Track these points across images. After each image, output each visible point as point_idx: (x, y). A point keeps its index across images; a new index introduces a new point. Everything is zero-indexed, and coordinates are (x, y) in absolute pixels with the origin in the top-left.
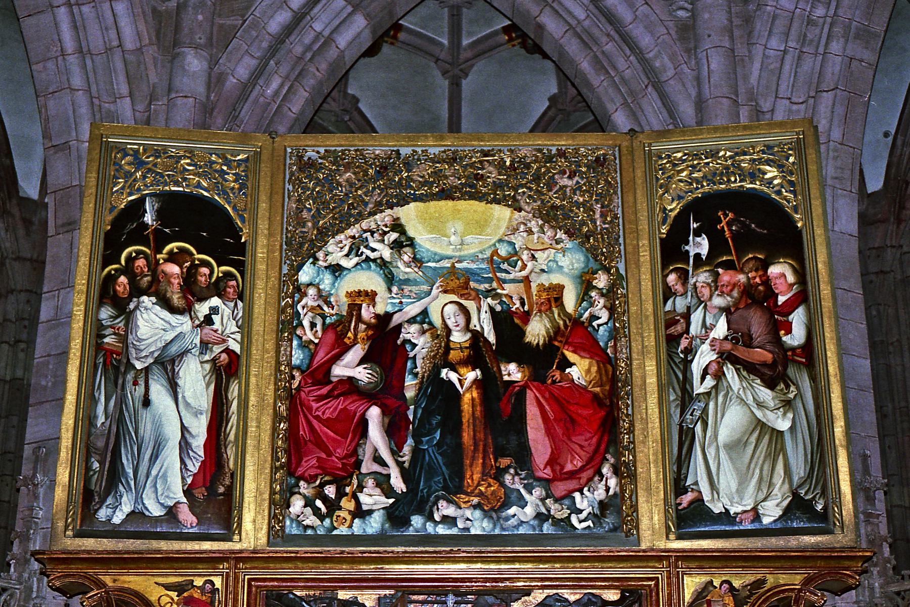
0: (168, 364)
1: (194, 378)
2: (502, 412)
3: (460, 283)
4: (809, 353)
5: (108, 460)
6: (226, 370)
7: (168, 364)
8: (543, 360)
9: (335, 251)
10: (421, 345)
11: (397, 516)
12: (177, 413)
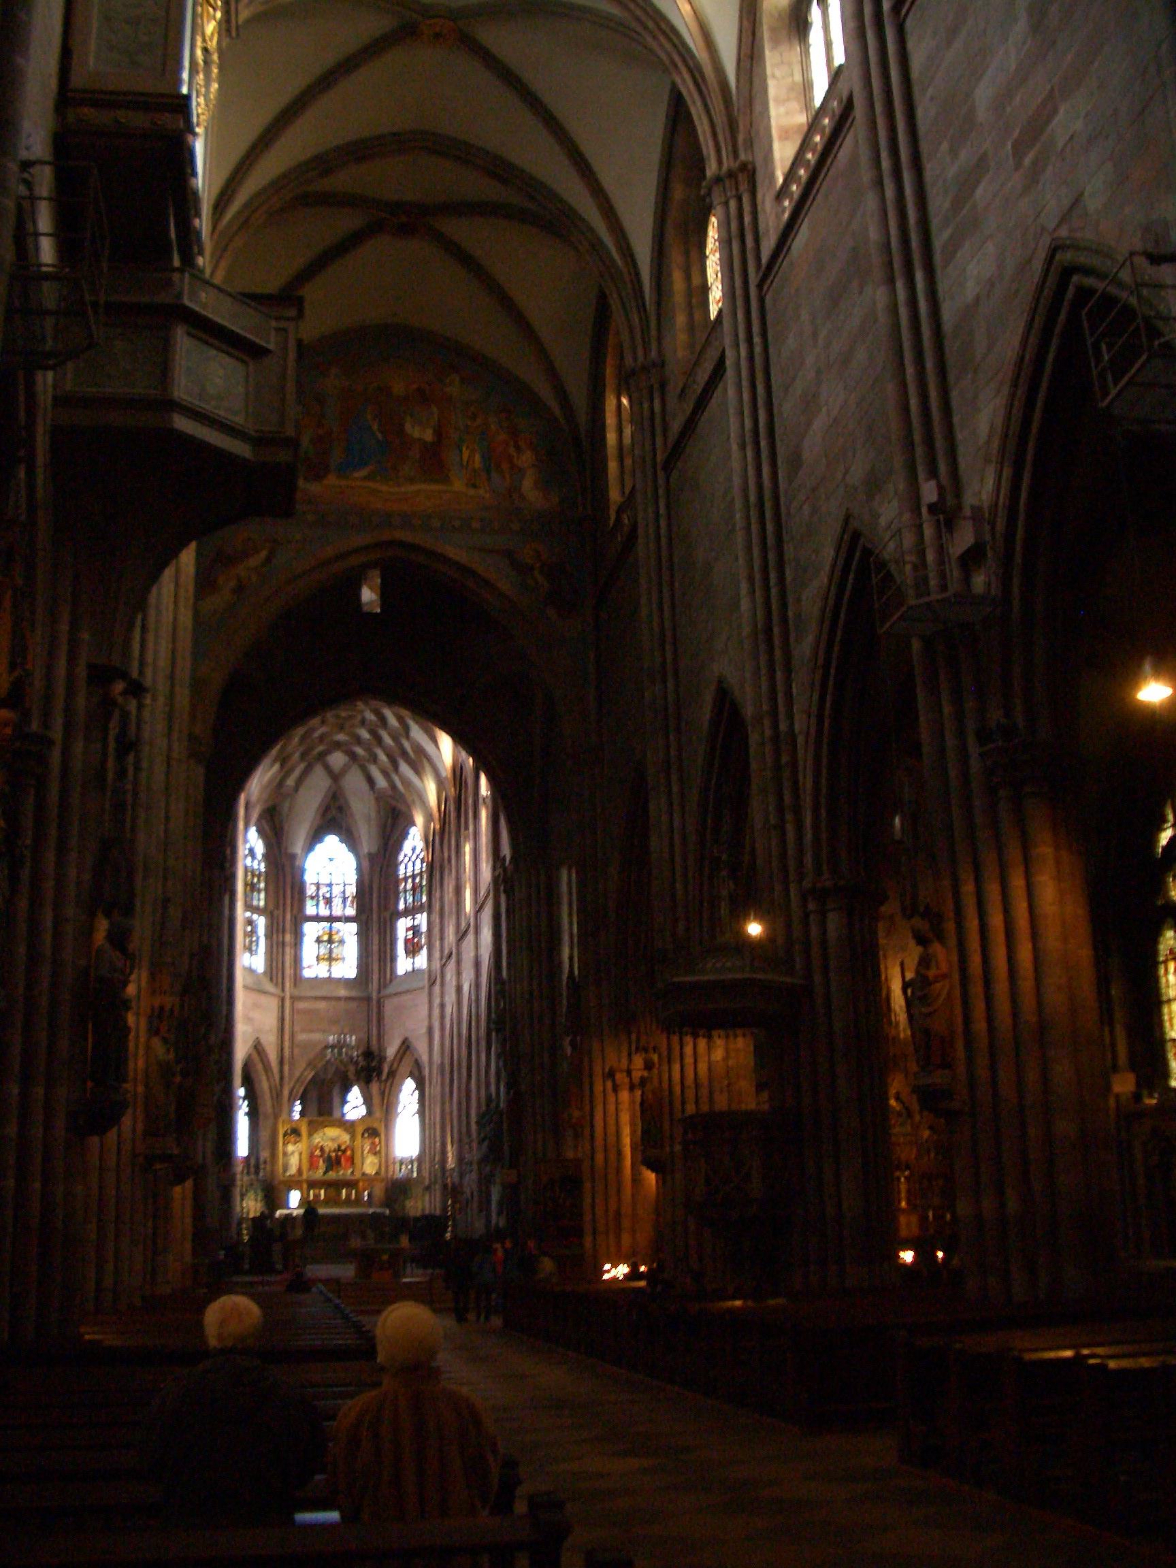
0: (293, 1153)
1: (296, 1156)
2: (338, 1162)
3: (333, 1140)
4: (380, 1152)
5: (286, 1167)
6: (301, 1154)
7: (293, 1153)
8: (344, 1151)
9: (315, 1136)
10: (327, 1150)
11: (325, 1173)
12: (294, 1161)
